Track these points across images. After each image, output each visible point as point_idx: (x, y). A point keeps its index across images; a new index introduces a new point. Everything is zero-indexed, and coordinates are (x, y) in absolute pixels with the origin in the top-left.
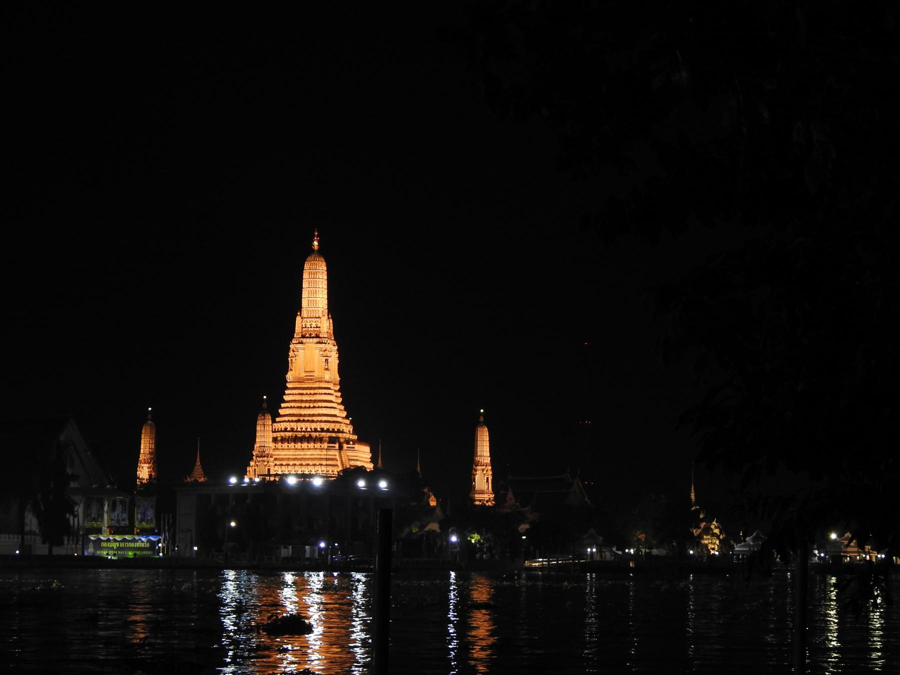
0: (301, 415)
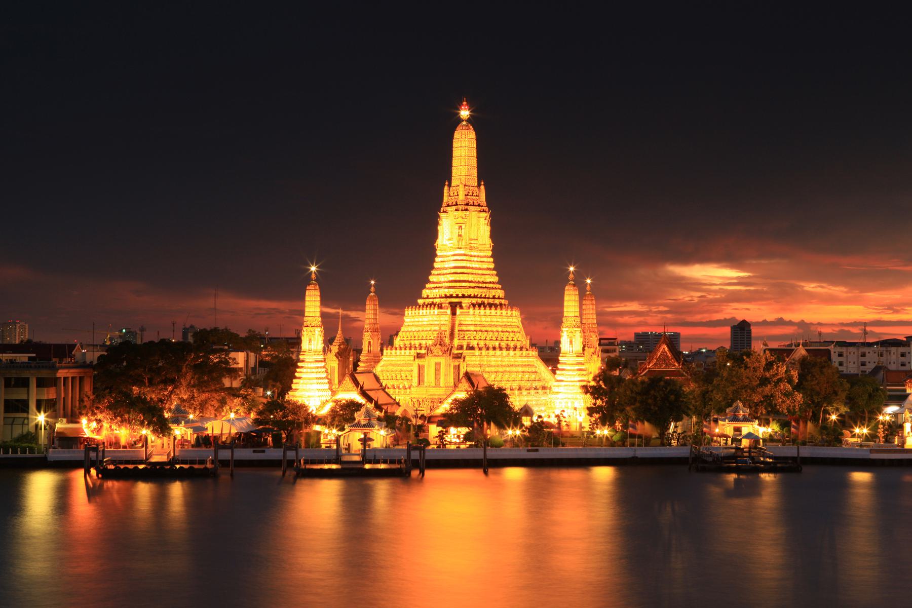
0: (439, 283)
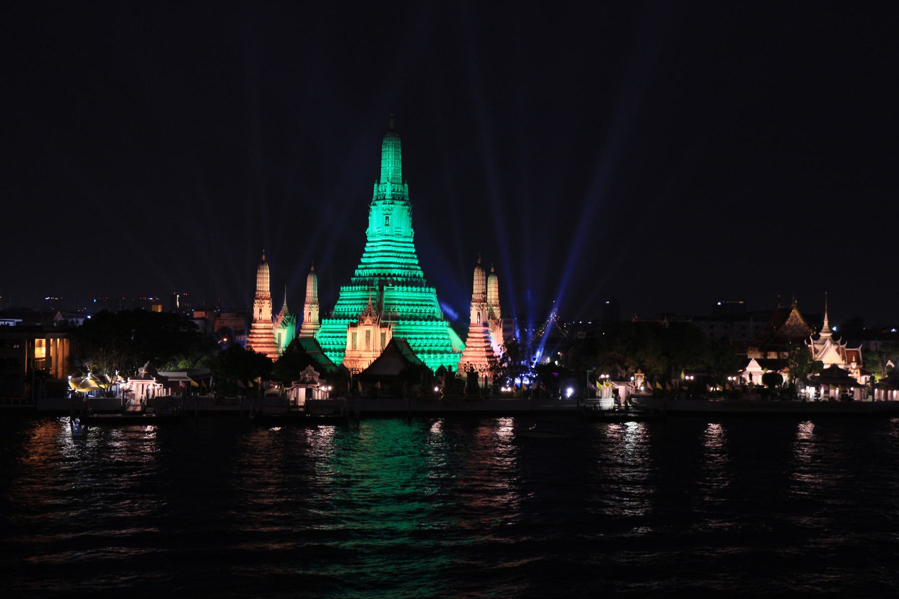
0: (369, 264)
